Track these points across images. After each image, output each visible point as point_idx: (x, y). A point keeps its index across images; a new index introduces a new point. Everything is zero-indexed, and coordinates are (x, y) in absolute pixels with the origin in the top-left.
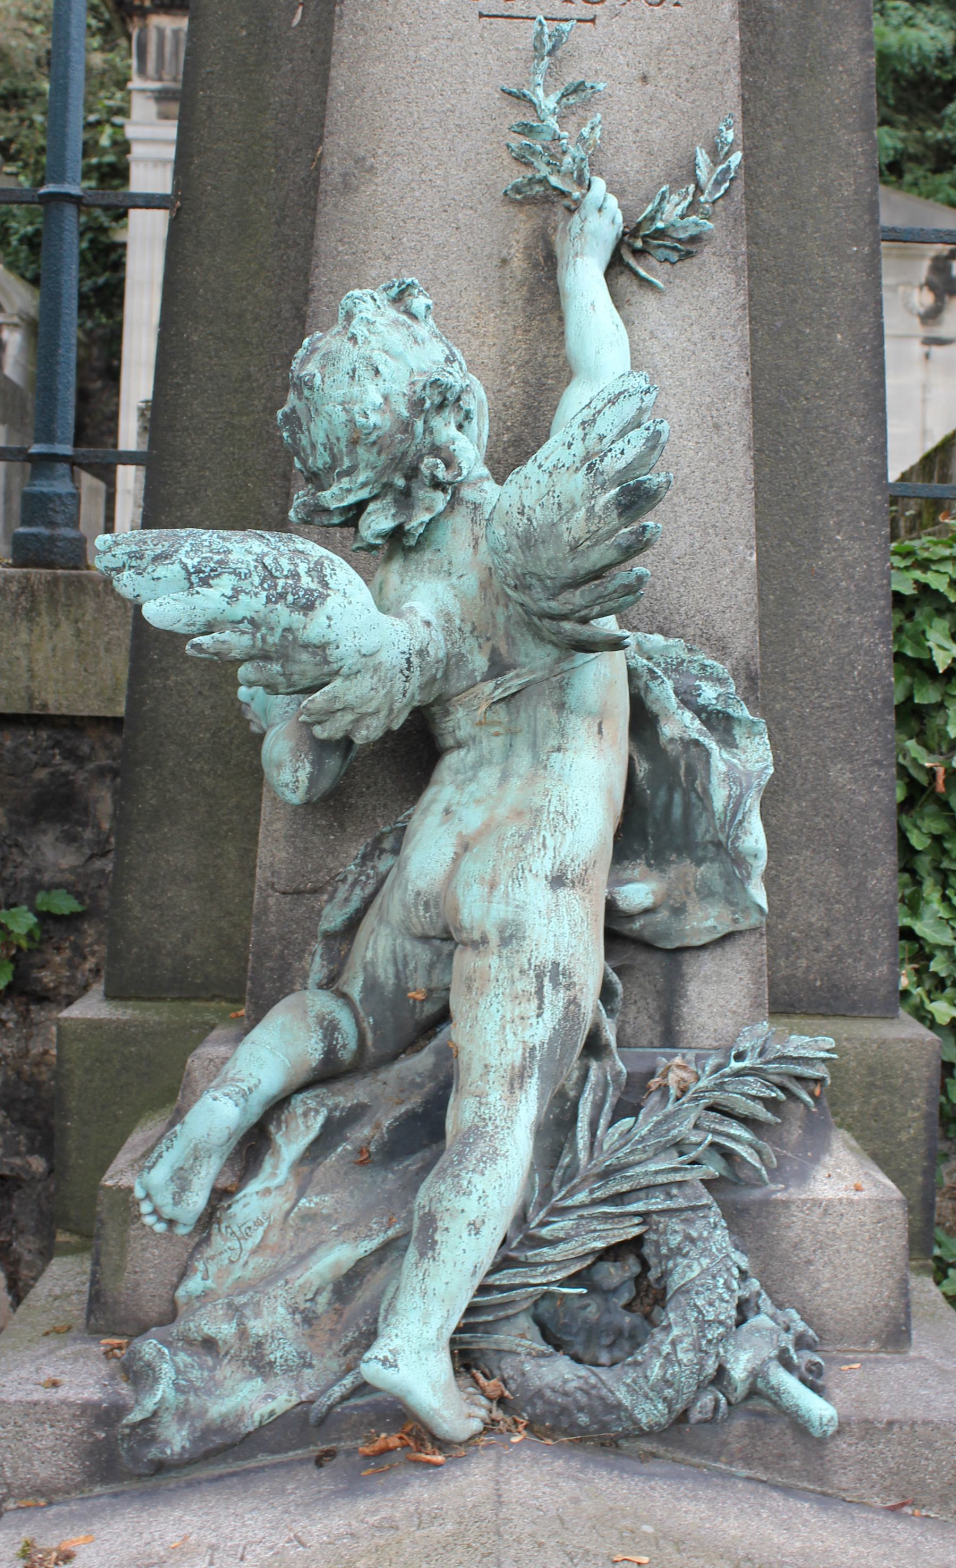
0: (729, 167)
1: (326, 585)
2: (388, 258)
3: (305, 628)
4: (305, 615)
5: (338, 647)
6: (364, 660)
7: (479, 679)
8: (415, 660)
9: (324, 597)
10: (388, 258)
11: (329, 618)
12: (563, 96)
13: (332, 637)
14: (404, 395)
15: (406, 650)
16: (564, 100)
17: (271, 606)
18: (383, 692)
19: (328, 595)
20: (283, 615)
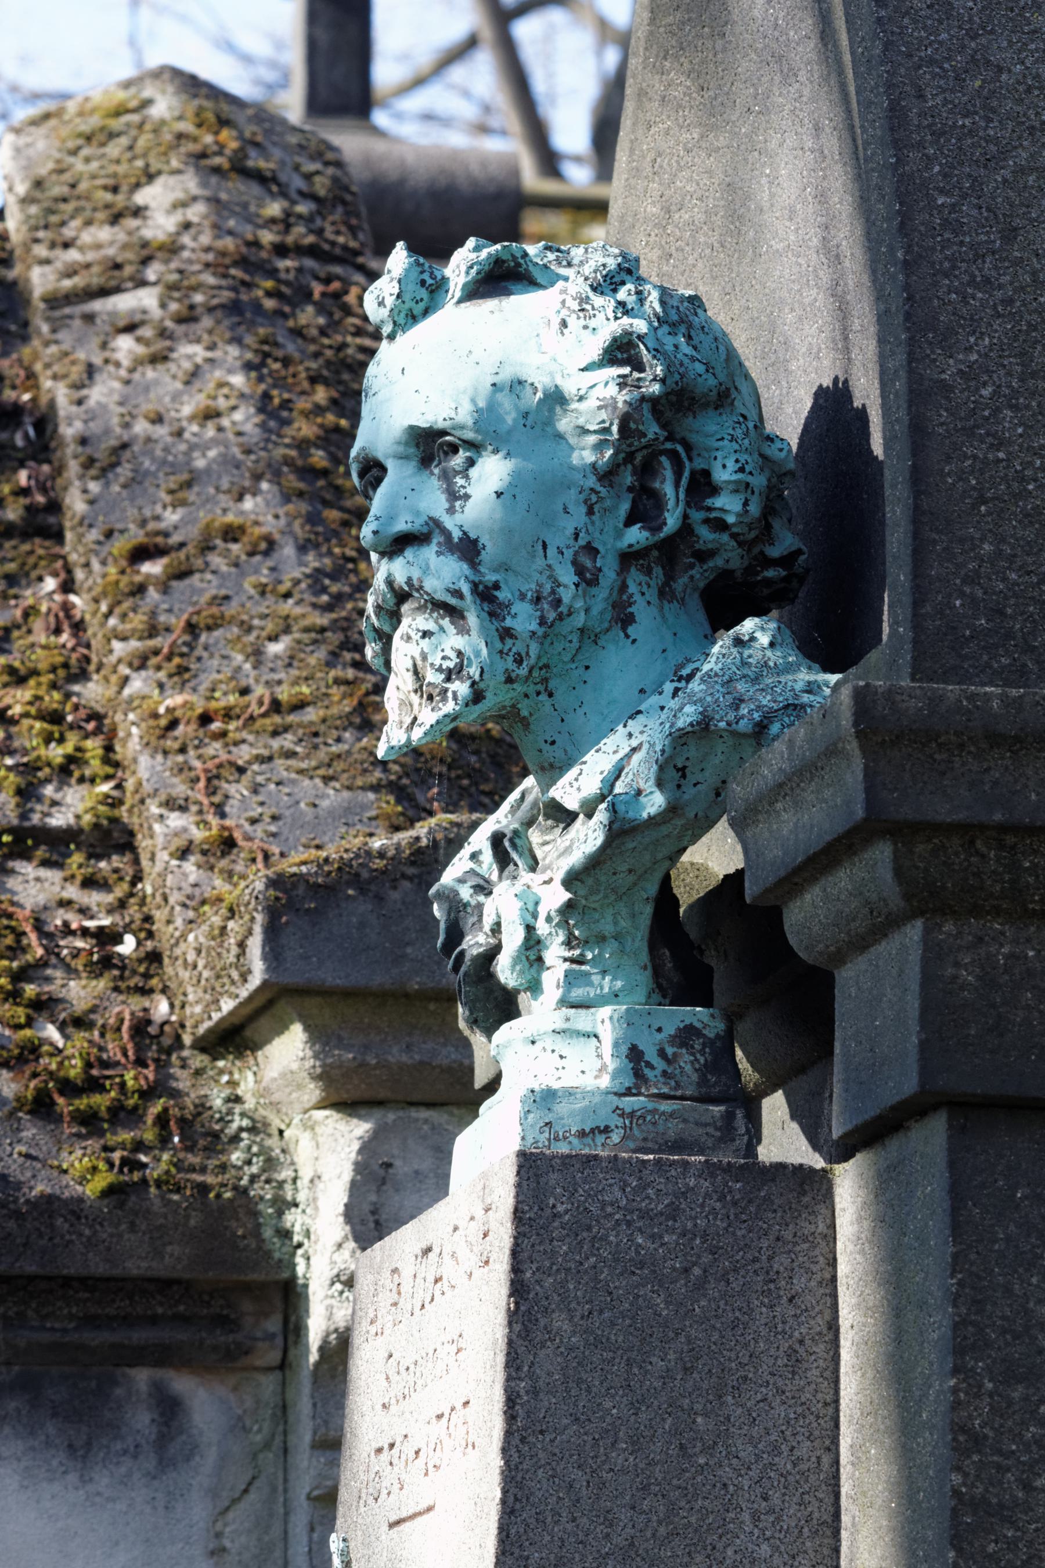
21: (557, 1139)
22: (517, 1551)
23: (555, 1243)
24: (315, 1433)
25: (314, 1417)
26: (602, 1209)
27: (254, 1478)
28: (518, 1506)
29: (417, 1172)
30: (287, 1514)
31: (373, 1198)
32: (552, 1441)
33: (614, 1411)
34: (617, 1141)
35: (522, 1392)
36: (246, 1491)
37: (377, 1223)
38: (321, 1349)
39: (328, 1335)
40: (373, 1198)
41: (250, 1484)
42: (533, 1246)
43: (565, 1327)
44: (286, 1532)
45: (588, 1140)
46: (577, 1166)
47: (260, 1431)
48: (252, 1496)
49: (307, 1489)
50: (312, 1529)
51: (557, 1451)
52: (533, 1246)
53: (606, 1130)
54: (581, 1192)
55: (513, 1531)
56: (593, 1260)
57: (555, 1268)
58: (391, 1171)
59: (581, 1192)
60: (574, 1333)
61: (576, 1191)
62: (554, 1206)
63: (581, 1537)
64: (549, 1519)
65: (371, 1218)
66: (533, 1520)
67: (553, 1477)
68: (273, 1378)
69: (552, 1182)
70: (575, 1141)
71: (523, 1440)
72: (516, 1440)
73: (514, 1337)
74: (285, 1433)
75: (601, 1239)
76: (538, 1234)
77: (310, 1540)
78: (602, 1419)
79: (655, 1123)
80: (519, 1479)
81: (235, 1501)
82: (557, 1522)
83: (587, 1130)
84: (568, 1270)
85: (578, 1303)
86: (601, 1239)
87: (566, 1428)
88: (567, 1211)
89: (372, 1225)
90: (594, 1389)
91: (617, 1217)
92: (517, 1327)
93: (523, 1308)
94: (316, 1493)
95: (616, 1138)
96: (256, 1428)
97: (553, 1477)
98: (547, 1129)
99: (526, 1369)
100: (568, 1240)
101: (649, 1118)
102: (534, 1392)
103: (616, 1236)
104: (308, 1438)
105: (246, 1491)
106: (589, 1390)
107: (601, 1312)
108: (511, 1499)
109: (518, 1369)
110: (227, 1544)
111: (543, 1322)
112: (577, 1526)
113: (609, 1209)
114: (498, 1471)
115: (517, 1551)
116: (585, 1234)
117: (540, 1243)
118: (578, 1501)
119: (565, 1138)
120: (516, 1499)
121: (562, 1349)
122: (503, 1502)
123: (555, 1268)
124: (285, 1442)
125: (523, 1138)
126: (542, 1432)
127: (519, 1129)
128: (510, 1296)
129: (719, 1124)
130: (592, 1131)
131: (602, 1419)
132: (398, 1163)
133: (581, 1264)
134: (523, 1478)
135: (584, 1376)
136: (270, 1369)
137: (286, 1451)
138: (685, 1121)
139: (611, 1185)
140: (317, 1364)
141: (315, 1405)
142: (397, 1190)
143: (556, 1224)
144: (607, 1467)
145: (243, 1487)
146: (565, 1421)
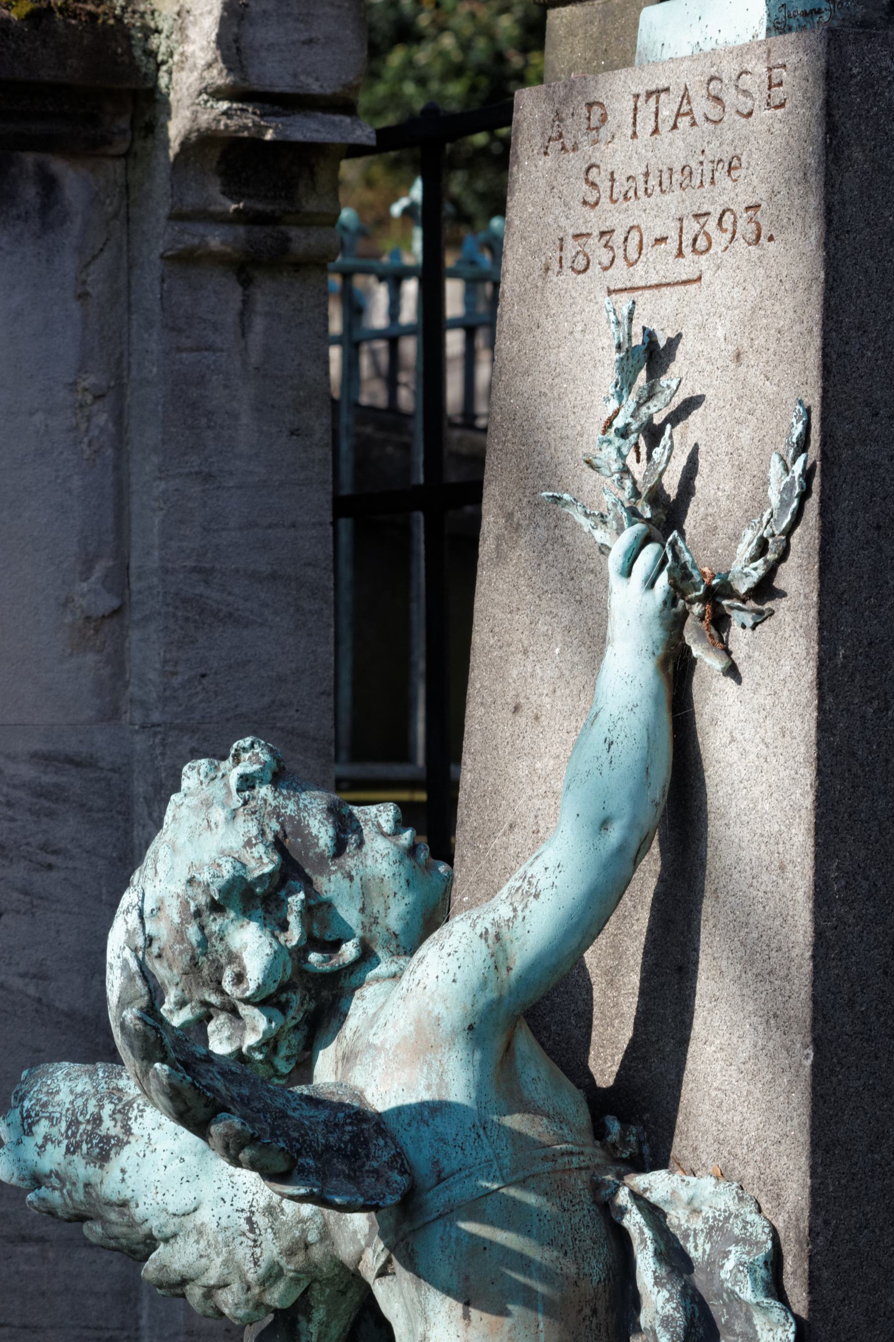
0: (794, 477)
1: (128, 1131)
2: (525, 652)
3: (101, 1182)
4: (101, 1167)
5: (137, 1206)
6: (176, 1220)
7: (363, 1243)
8: (261, 1220)
9: (121, 1144)
10: (525, 652)
11: (123, 1171)
12: (639, 405)
13: (128, 1194)
14: (178, 896)
15: (246, 1207)
16: (644, 410)
17: (69, 1157)
18: (218, 1261)
19: (128, 1142)
20: (82, 1169)
21: (789, 17)
22: (835, 317)
23: (853, 96)
24: (172, 207)
25: (172, 196)
26: (880, 72)
27: (108, 239)
28: (835, 285)
29: (265, 12)
30: (130, 268)
31: (235, 30)
32: (854, 239)
33: (891, 219)
34: (827, 20)
35: (836, 202)
36: (102, 250)
37: (238, 49)
38: (183, 144)
39: (190, 132)
40: (235, 30)
41: (105, 244)
42: (839, 98)
43: (860, 157)
44: (129, 282)
45: (809, 18)
46: (864, 40)
47: (111, 204)
48: (106, 254)
49: (161, 250)
50: (163, 281)
51: (857, 246)
52: (839, 98)
53: (819, 12)
54: (867, 60)
55: (832, 303)
56: (875, 109)
57: (853, 114)
58: (247, 10)
59: (867, 60)
60: (865, 161)
61: (864, 58)
62: (851, 69)
63: (874, 308)
64: (854, 294)
65: (234, 46)
66: (844, 295)
67: (855, 264)
68: (119, 164)
69: (850, 52)
70: (801, 19)
71: (837, 237)
72: (832, 238)
73: (829, 163)
74: (128, 206)
75: (880, 95)
76: (842, 89)
77: (162, 289)
78: (884, 224)
79: (848, 8)
80: (835, 265)
81: (95, 257)
82: (858, 297)
83: (808, 11)
84: (861, 116)
85: (868, 140)
86: (880, 95)
87: (862, 229)
88: (859, 73)
89: (234, 51)
90: (879, 203)
91: (889, 79)
92: (831, 156)
93: (834, 142)
94: (169, 253)
95: (826, 18)
96: (108, 201)
97: (855, 264)
98: (783, 9)
99: (837, 186)
100: (860, 95)
101: (845, 4)
102: (843, 203)
103: (889, 92)
104: (164, 211)
105: (102, 250)
106: (875, 204)
107: (881, 147)
108: (831, 280)
109: (833, 186)
110: (90, 290)
111: (847, 153)
112: (871, 300)
113: (884, 73)
114: (821, 259)
115: (835, 317)
116: (870, 90)
117: (843, 96)
118: (871, 282)
119: (795, 16)
120: (834, 280)
121: (859, 173)
122: (826, 281)
123: (853, 114)
124: (128, 213)
125: (769, 15)
126: (848, 232)
127: (765, 8)
128: (826, 134)
129: (887, 10)
130: (811, 11)
131: (884, 224)
132: (252, 4)
133: (869, 112)
134: (838, 265)
135: (872, 193)
136: (118, 157)
137: (128, 220)
138: (866, 7)
139: (885, 56)
140: (177, 156)
141: (172, 186)
142: (251, 25)
143: (852, 82)
144: (887, 258)
145: (100, 246)
146: (862, 225)
